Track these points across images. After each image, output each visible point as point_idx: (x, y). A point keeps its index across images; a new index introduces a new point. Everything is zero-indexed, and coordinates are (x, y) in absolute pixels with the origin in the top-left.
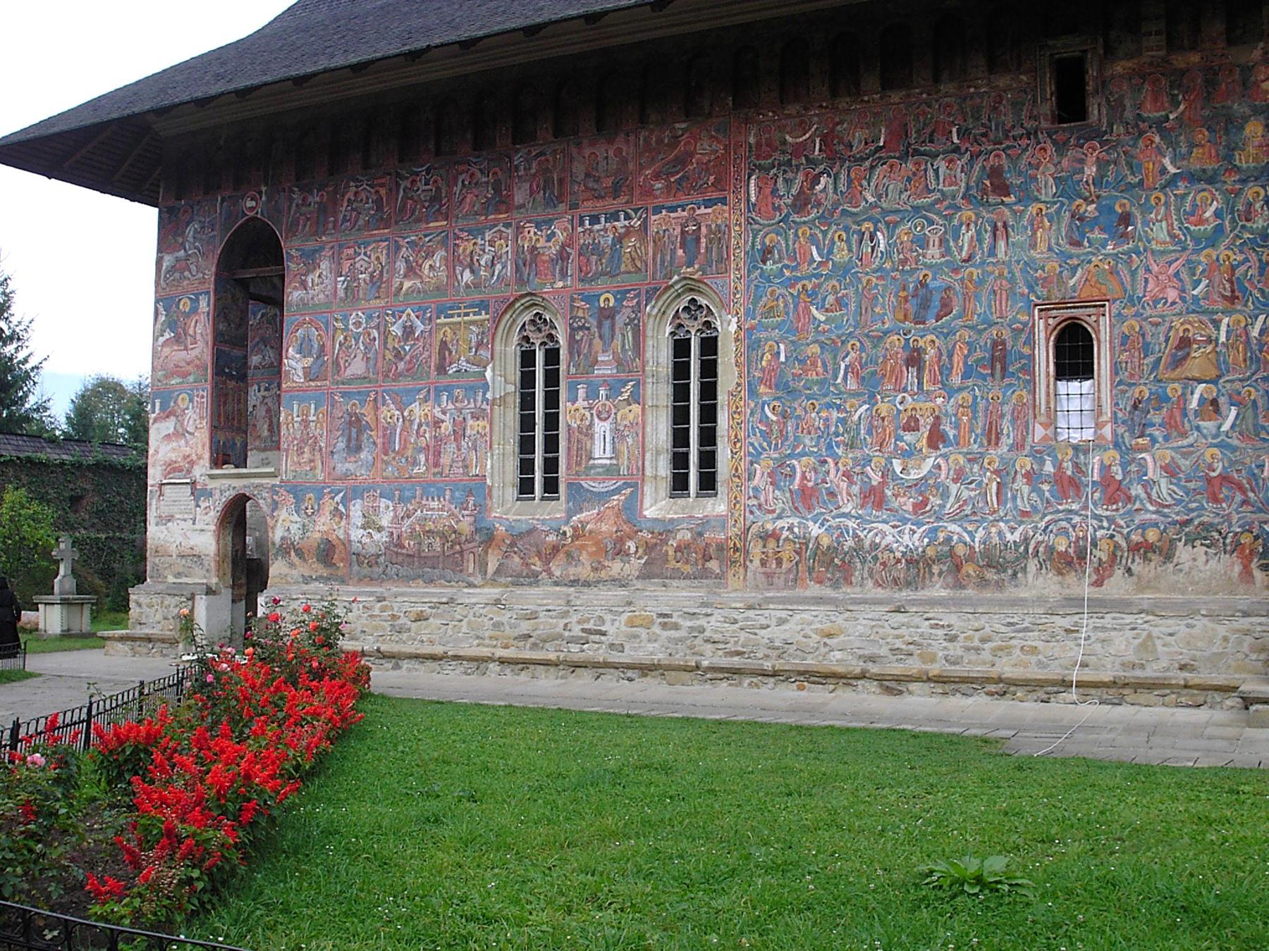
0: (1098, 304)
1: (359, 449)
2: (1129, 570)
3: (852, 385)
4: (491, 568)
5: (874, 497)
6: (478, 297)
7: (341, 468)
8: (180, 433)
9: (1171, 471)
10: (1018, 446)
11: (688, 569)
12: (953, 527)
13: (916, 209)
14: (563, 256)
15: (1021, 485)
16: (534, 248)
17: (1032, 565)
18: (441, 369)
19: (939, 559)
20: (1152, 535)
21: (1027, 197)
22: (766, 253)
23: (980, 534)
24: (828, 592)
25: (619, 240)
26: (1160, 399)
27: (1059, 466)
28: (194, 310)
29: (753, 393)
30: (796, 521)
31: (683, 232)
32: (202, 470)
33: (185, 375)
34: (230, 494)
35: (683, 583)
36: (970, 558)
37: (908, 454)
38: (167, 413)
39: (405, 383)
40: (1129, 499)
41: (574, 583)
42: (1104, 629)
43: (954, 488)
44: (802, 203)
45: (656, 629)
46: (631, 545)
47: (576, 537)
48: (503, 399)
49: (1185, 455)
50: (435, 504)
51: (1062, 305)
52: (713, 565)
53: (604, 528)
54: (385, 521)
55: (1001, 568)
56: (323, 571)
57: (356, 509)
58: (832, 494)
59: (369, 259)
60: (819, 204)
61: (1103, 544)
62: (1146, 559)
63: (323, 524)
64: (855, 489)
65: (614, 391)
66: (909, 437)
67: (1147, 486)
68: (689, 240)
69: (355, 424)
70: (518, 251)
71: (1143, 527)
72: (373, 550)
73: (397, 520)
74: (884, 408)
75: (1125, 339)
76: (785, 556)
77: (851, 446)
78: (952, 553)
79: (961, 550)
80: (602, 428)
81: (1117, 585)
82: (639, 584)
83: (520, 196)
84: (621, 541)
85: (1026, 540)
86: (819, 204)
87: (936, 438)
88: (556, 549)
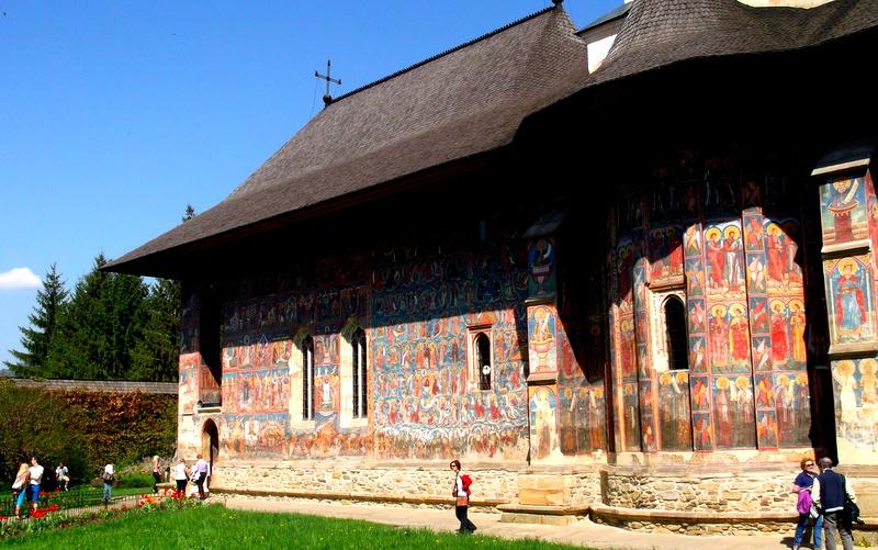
0: (488, 326)
1: (248, 398)
2: (502, 450)
3: (407, 366)
4: (291, 450)
5: (415, 417)
6: (285, 328)
7: (243, 406)
8: (189, 392)
9: (514, 403)
10: (462, 393)
11: (355, 451)
12: (441, 430)
13: (428, 284)
14: (313, 309)
15: (464, 410)
16: (304, 306)
17: (469, 447)
18: (274, 361)
19: (437, 445)
20: (509, 433)
21: (464, 278)
22: (378, 306)
23: (451, 434)
24: (397, 460)
25: (331, 301)
26: (510, 369)
27: (476, 402)
28: (193, 335)
29: (375, 370)
30: (390, 428)
31: (352, 298)
32: (196, 408)
33: (190, 364)
34: (206, 419)
35: (354, 458)
36: (448, 445)
37: (426, 397)
38: (185, 382)
39: (262, 368)
40: (501, 416)
41: (318, 458)
42: (489, 477)
43: (441, 412)
44: (390, 283)
45: (342, 479)
46: (336, 440)
47: (319, 437)
48: (296, 374)
49: (519, 395)
50: (272, 422)
51: (477, 327)
52: (363, 449)
53: (328, 432)
54: (256, 430)
55: (457, 449)
56: (236, 454)
57: (247, 424)
58: (401, 416)
59: (250, 312)
60: (395, 284)
61: (492, 438)
62: (507, 445)
63: (236, 432)
64: (409, 414)
65: (330, 371)
66: (426, 389)
67: (507, 409)
68: (353, 300)
69: (246, 385)
70: (298, 306)
71: (505, 429)
72: (252, 444)
73: (261, 430)
74: (418, 376)
75: (498, 341)
76: (387, 444)
77: (407, 394)
78: (442, 443)
79: (445, 441)
80: (326, 387)
81: (498, 457)
82: (339, 458)
83: (299, 283)
84: (333, 438)
85: (467, 436)
86: (395, 284)
87: (435, 390)
88: (312, 443)
